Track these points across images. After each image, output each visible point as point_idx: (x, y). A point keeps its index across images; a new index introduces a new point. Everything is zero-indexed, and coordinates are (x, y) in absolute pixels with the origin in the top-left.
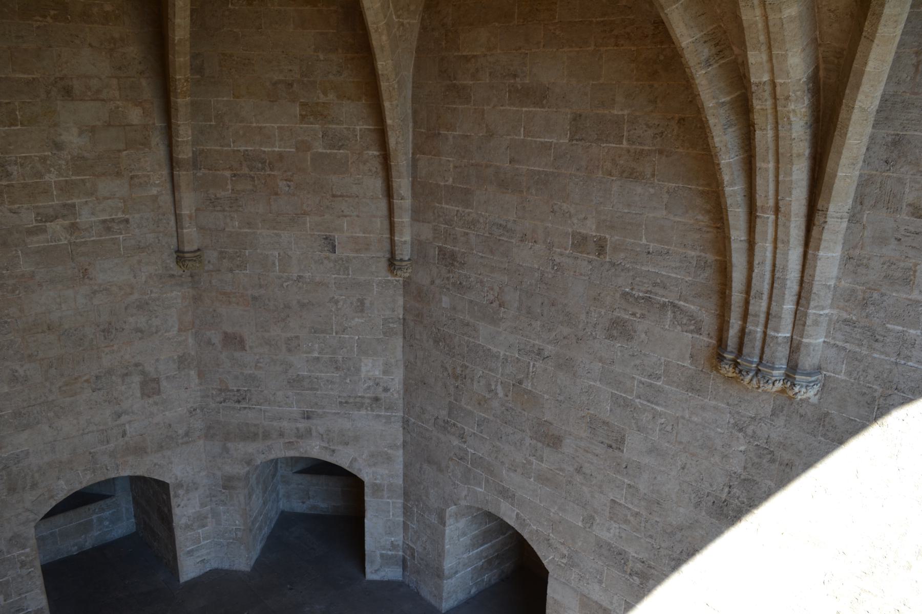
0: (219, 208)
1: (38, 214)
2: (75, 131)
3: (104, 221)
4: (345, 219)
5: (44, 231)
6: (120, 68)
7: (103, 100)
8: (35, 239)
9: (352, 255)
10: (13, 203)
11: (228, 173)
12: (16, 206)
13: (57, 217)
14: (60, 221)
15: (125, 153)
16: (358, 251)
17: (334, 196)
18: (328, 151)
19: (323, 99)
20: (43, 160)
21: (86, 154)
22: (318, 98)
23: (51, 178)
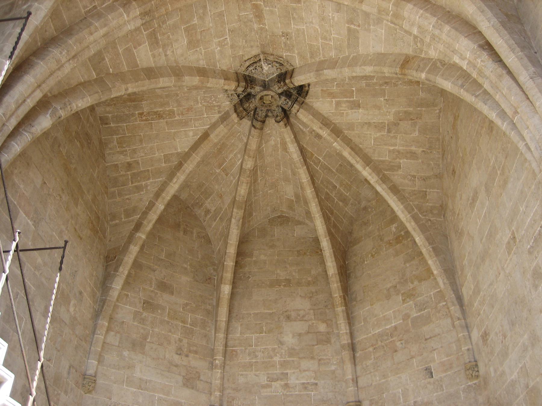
0: (368, 372)
1: (268, 377)
2: (291, 335)
3: (303, 384)
4: (435, 352)
5: (270, 386)
6: (315, 305)
7: (306, 320)
8: (265, 390)
9: (443, 375)
10: (257, 371)
11: (371, 349)
12: (258, 372)
13: (278, 380)
14: (279, 382)
15: (316, 346)
16: (445, 371)
17: (426, 340)
18: (419, 314)
19: (412, 286)
20: (274, 350)
21: (295, 347)
22: (410, 287)
23: (277, 359)
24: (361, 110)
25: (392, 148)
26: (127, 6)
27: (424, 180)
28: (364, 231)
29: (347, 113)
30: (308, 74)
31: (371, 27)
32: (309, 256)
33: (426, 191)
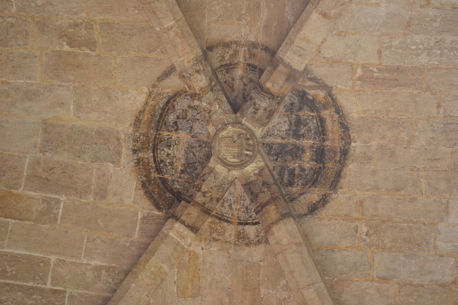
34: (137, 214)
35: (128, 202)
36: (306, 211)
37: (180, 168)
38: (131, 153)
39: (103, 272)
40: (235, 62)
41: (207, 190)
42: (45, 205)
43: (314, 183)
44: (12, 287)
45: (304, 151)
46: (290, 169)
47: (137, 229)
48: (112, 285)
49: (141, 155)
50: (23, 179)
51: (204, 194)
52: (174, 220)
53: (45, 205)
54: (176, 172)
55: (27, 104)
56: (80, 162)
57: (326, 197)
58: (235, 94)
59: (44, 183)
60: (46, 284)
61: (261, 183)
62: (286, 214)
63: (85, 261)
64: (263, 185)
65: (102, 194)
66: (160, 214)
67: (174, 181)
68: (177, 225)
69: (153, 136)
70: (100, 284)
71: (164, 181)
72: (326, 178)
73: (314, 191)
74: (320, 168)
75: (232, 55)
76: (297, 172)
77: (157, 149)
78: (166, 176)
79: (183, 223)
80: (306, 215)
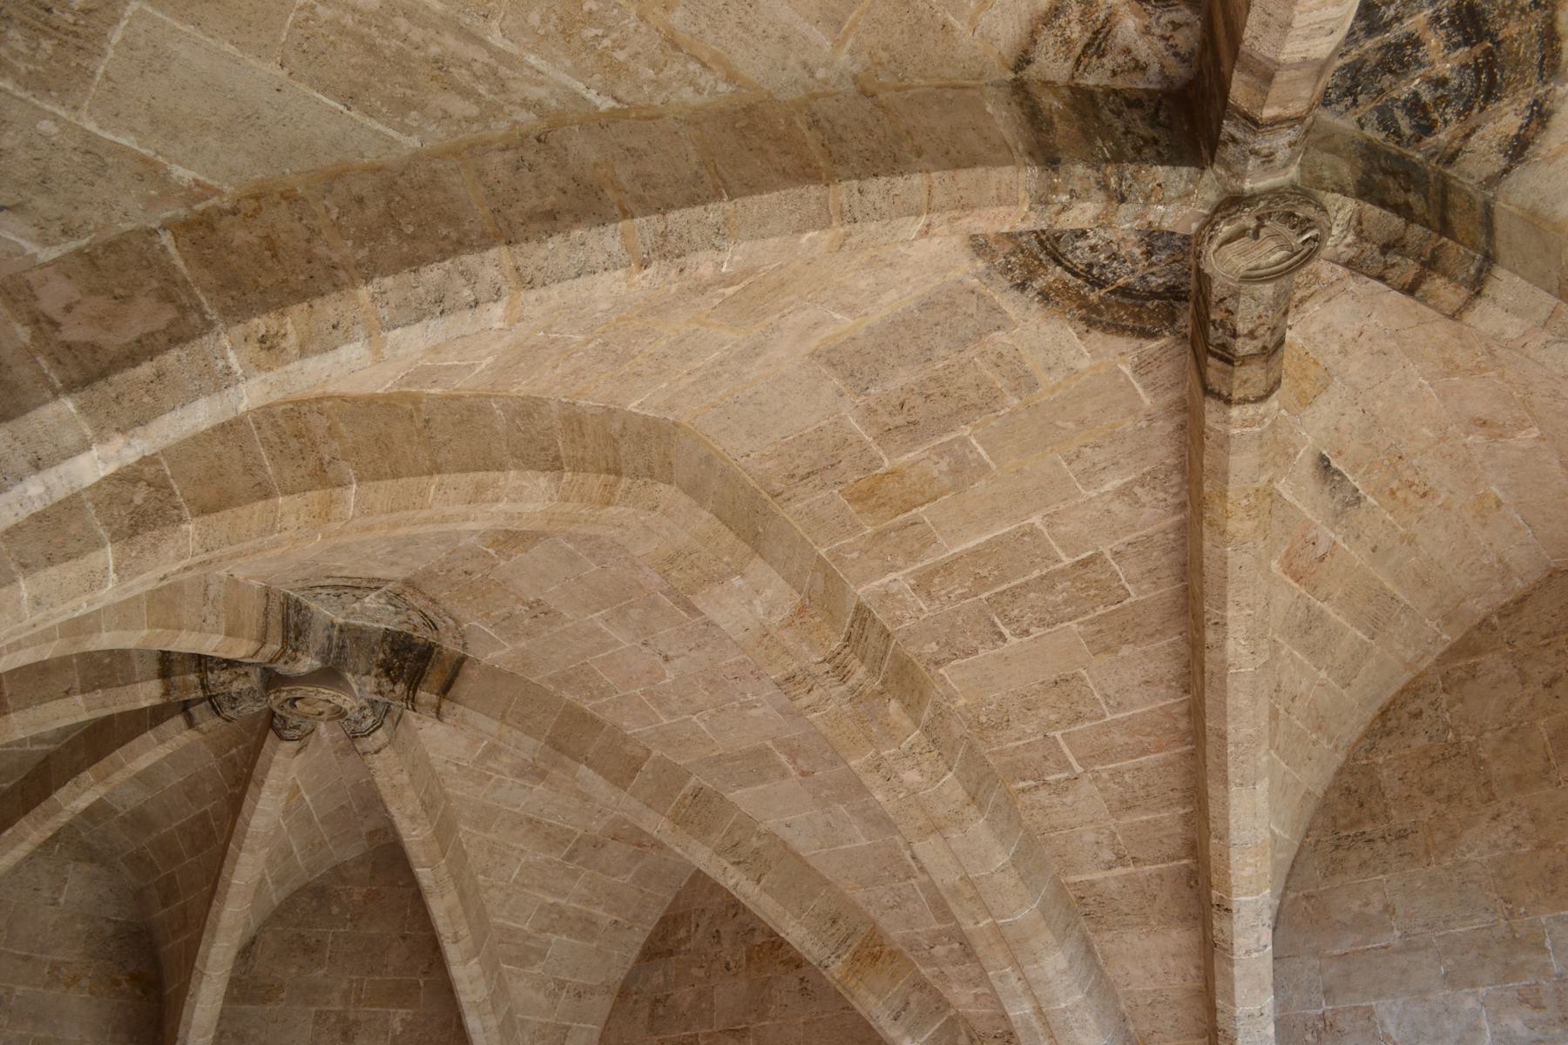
24: (539, 787)
25: (550, 900)
26: (146, 539)
27: (579, 995)
28: (293, 970)
29: (498, 781)
30: (517, 734)
31: (842, 808)
32: (86, 995)
33: (568, 1028)
34: (1119, 371)
35: (1084, 364)
36: (1503, 163)
37: (1137, 251)
38: (1017, 293)
39: (1138, 490)
40: (1102, 17)
41: (1251, 326)
42: (947, 459)
43: (1491, 92)
44: (1014, 594)
45: (1415, 42)
46: (1406, 101)
47: (1140, 390)
48: (1170, 500)
49: (1039, 284)
50: (874, 447)
51: (1252, 335)
52: (1221, 403)
53: (947, 459)
54: (1135, 262)
55: (760, 361)
56: (940, 365)
57: (1541, 106)
58: (1155, 68)
59: (913, 430)
60: (1058, 561)
61: (1376, 254)
62: (1480, 271)
63: (1093, 494)
64: (1383, 253)
65: (1024, 382)
66: (1163, 341)
67: (1143, 278)
68: (1235, 412)
69: (1035, 243)
70: (1147, 512)
71: (1125, 291)
72: (1518, 63)
73: (1499, 109)
74: (1488, 53)
75: (1083, 14)
76: (1426, 97)
77: (1063, 255)
78: (1121, 282)
79: (1244, 401)
80: (1506, 171)
